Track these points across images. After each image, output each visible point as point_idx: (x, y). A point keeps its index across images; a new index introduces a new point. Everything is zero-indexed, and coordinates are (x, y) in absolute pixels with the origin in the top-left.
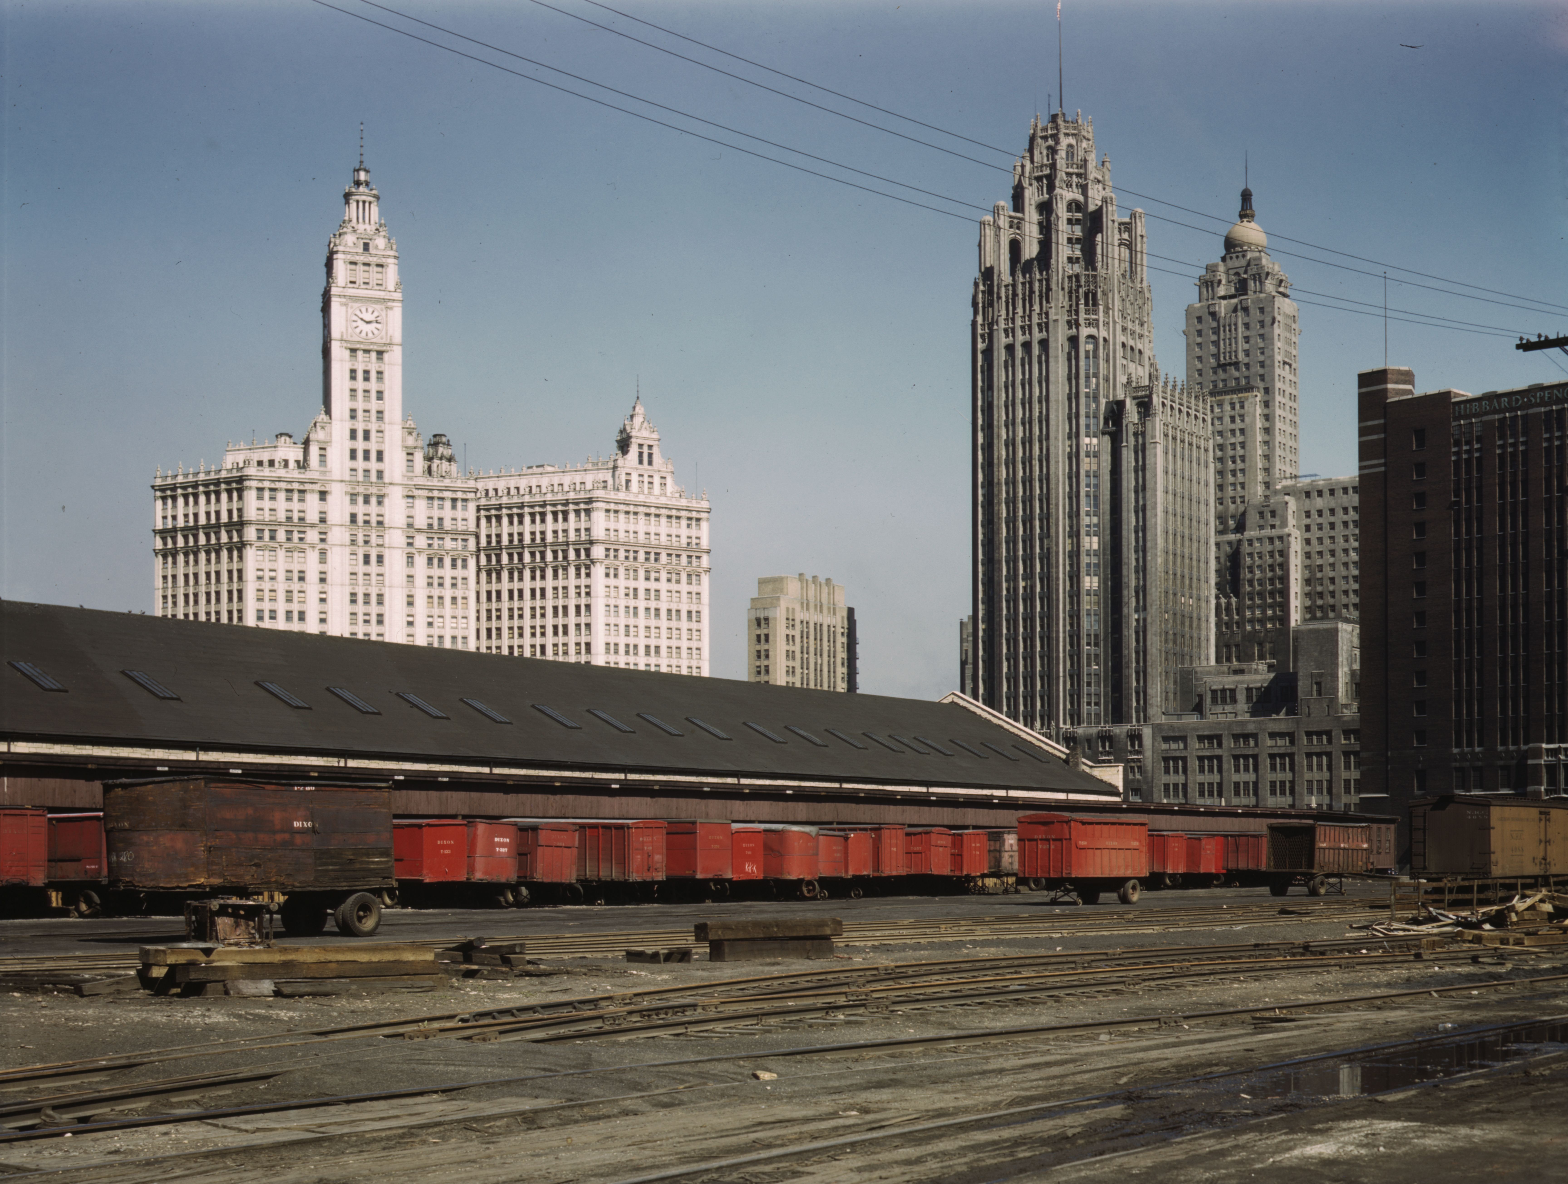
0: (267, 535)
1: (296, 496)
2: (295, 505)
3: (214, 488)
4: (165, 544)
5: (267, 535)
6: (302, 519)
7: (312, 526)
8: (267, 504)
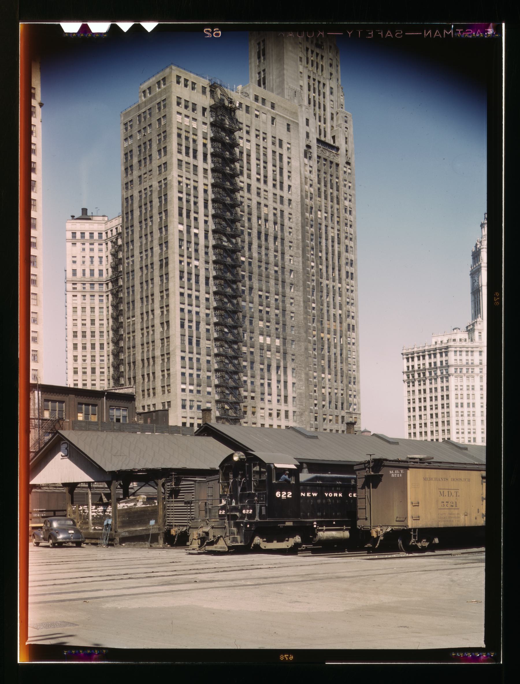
0: (459, 370)
3: (433, 353)
4: (409, 378)
5: (459, 370)
6: (472, 363)
7: (477, 366)
8: (458, 357)
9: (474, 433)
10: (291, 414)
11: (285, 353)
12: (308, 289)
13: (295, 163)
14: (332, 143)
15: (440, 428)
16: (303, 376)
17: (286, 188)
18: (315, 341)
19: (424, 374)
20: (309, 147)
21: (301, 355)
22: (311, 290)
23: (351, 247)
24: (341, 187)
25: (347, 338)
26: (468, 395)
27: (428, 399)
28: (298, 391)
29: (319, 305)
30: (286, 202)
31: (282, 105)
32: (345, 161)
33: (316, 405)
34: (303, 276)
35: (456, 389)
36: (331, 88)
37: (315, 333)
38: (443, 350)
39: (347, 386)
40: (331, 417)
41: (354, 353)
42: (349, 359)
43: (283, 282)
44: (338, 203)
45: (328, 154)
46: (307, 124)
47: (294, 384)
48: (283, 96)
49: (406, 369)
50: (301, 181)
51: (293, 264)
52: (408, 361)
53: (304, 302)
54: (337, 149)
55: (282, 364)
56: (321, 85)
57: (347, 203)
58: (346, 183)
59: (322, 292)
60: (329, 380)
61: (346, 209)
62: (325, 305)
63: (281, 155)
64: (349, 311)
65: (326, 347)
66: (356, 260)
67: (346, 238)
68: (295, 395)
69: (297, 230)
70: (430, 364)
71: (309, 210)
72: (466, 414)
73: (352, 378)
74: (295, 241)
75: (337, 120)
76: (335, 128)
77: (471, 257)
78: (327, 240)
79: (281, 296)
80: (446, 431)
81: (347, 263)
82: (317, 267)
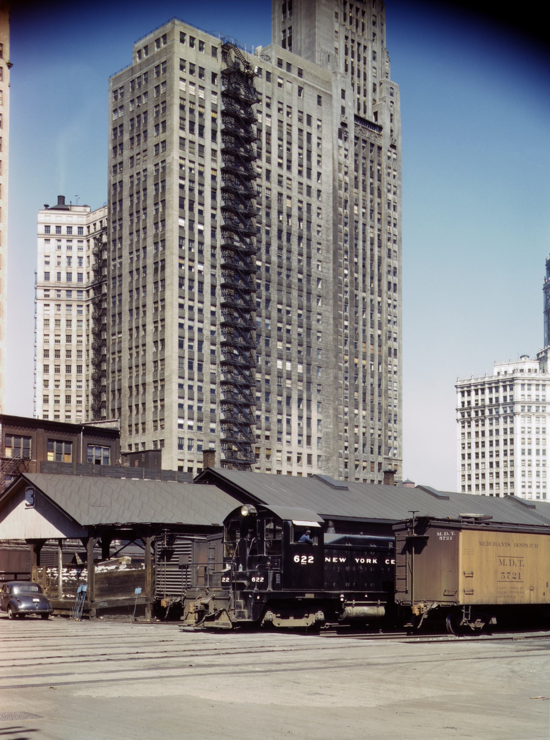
0: (526, 408)
1: (541, 387)
2: (541, 393)
3: (494, 386)
4: (463, 416)
5: (526, 408)
6: (544, 400)
8: (526, 392)
9: (544, 487)
10: (314, 459)
11: (309, 383)
12: (339, 303)
13: (327, 145)
14: (373, 121)
15: (502, 480)
16: (331, 411)
17: (314, 175)
18: (346, 368)
19: (483, 412)
20: (344, 125)
21: (329, 385)
22: (343, 304)
23: (395, 251)
24: (385, 177)
25: (387, 365)
26: (538, 439)
27: (487, 444)
28: (325, 430)
29: (353, 323)
30: (314, 193)
31: (313, 72)
32: (390, 144)
33: (346, 448)
34: (334, 286)
35: (523, 432)
36: (374, 52)
37: (347, 358)
38: (508, 383)
39: (386, 425)
40: (365, 464)
41: (395, 384)
42: (389, 392)
43: (309, 293)
44: (380, 196)
45: (368, 134)
46: (343, 97)
47: (319, 421)
48: (313, 61)
49: (460, 406)
50: (334, 167)
51: (322, 271)
52: (463, 396)
53: (334, 319)
54: (380, 128)
55: (305, 396)
56: (362, 48)
57: (391, 196)
58: (390, 171)
59: (357, 307)
60: (364, 417)
61: (389, 204)
62: (361, 323)
63: (309, 135)
64: (390, 332)
65: (361, 375)
66: (401, 267)
67: (389, 239)
68: (320, 436)
69: (328, 229)
70: (491, 399)
71: (343, 204)
72: (534, 463)
73: (393, 416)
74: (324, 243)
75: (381, 92)
76: (378, 103)
77: (545, 267)
78: (364, 241)
79: (305, 311)
80: (509, 484)
81: (389, 272)
82: (352, 275)
